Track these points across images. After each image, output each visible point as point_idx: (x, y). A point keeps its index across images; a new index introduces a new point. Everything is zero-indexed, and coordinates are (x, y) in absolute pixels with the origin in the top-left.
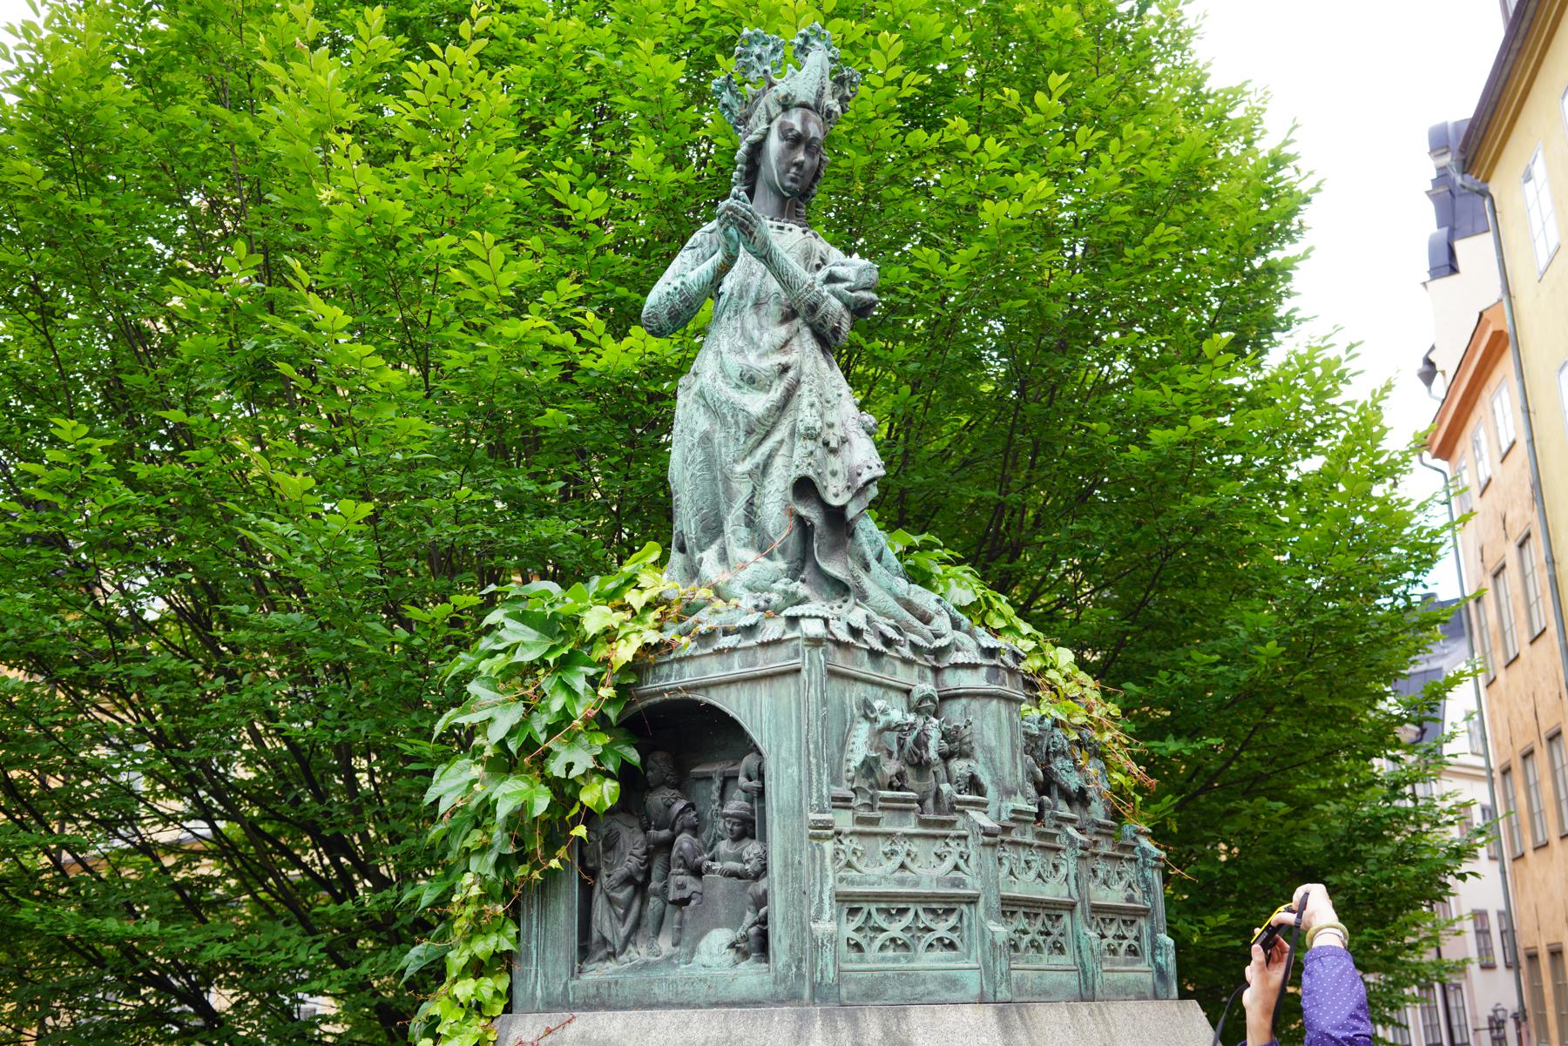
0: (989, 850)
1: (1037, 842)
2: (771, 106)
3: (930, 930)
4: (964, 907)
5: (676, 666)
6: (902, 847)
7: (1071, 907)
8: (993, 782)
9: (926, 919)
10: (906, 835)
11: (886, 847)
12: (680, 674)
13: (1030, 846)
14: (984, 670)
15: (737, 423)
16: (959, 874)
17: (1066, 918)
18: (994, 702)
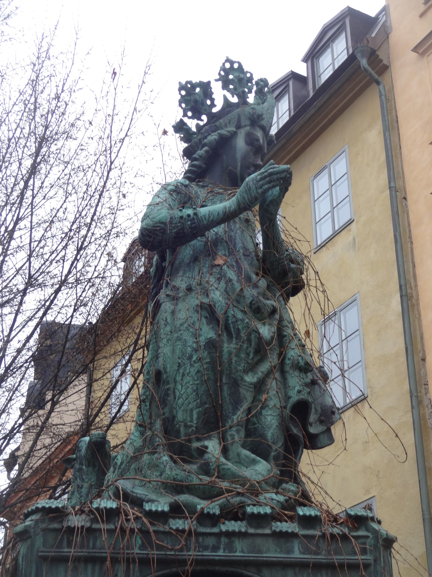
2: (243, 118)
5: (224, 540)
12: (230, 548)
15: (249, 340)
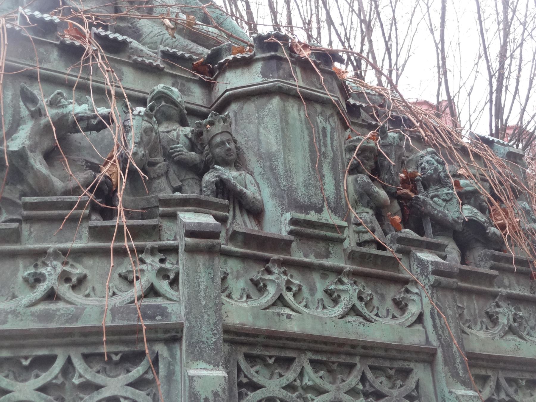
0: (201, 260)
1: (348, 267)
3: (98, 387)
4: (161, 349)
6: (51, 271)
7: (427, 357)
8: (274, 195)
9: (83, 371)
10: (64, 252)
11: (25, 270)
13: (338, 271)
14: (258, 67)
16: (159, 301)
17: (420, 373)
18: (276, 101)
